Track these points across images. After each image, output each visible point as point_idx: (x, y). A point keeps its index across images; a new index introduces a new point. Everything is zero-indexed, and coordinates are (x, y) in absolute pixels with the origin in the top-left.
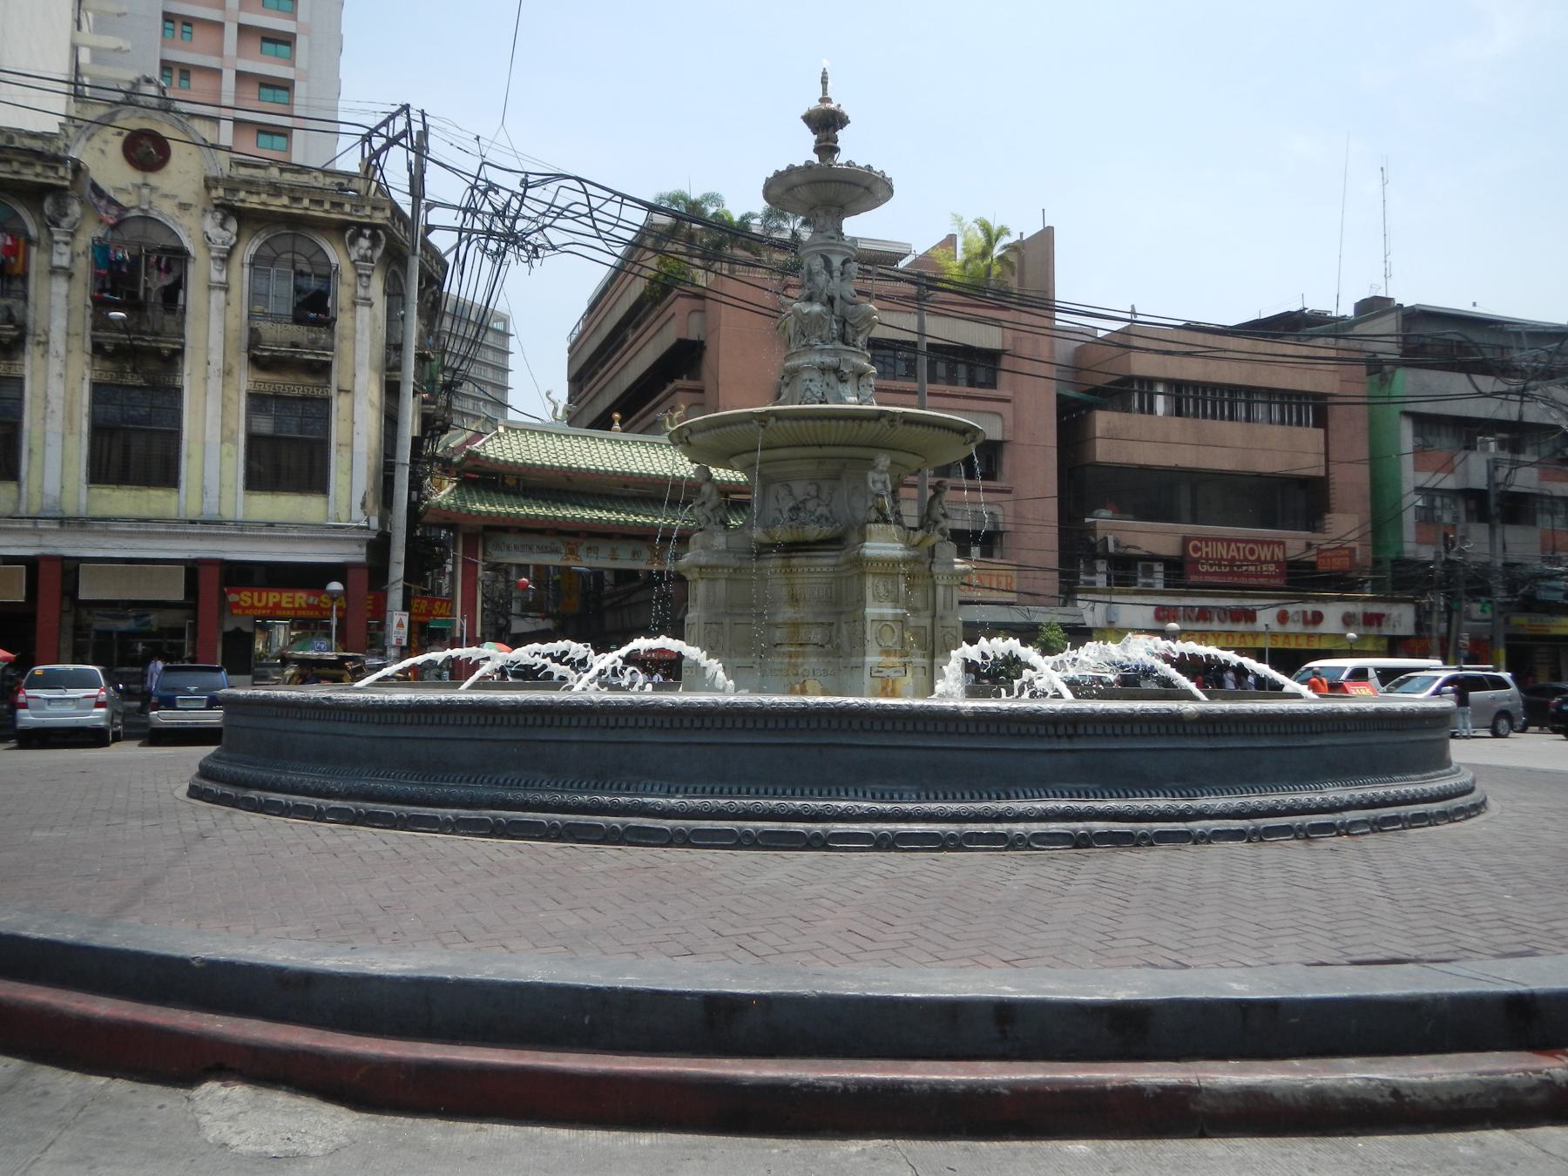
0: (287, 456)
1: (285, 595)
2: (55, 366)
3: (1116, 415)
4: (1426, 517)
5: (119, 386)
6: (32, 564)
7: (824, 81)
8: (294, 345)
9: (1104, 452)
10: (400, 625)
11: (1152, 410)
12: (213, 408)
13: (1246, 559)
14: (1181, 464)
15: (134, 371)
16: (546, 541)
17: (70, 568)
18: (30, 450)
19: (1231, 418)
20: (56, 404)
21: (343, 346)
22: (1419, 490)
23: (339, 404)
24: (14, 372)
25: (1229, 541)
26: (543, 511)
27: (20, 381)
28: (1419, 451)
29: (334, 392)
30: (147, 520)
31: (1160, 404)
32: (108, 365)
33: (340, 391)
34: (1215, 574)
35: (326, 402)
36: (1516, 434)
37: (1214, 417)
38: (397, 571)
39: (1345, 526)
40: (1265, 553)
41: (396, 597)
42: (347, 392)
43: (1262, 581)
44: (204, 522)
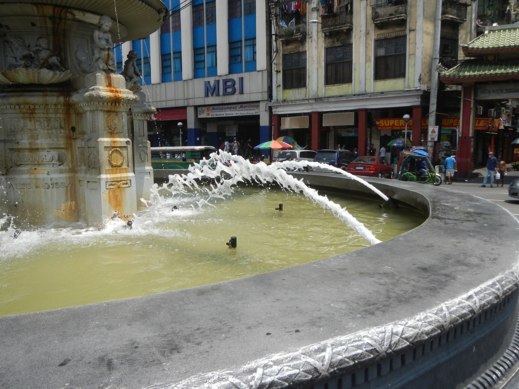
0: (390, 63)
1: (396, 121)
2: (314, 44)
5: (334, 47)
6: (310, 115)
8: (391, 15)
10: (433, 132)
12: (362, 49)
15: (337, 41)
16: (511, 86)
17: (320, 114)
18: (309, 76)
20: (315, 58)
21: (413, 9)
23: (410, 37)
24: (304, 50)
26: (503, 71)
27: (305, 52)
29: (407, 31)
30: (342, 96)
32: (330, 40)
33: (410, 31)
35: (405, 36)
38: (433, 108)
41: (432, 119)
42: (414, 30)
44: (359, 95)
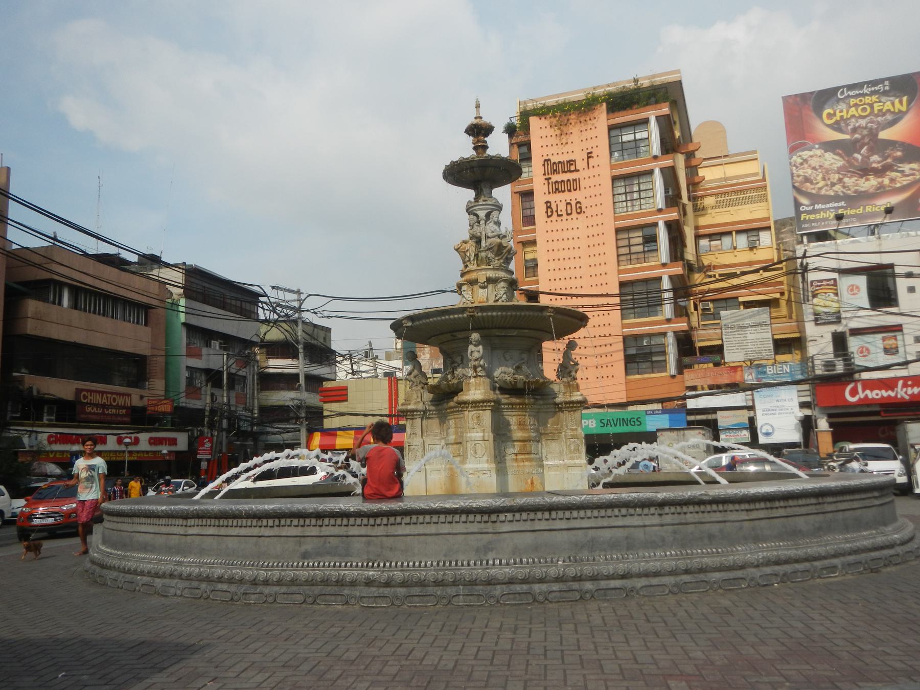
3: (41, 304)
4: (190, 381)
7: (478, 106)
9: (31, 328)
11: (60, 304)
13: (111, 405)
14: (77, 341)
19: (104, 315)
22: (187, 367)
25: (103, 393)
28: (188, 344)
31: (66, 301)
34: (94, 414)
36: (227, 340)
37: (95, 313)
39: (157, 385)
40: (121, 401)
43: (119, 418)
